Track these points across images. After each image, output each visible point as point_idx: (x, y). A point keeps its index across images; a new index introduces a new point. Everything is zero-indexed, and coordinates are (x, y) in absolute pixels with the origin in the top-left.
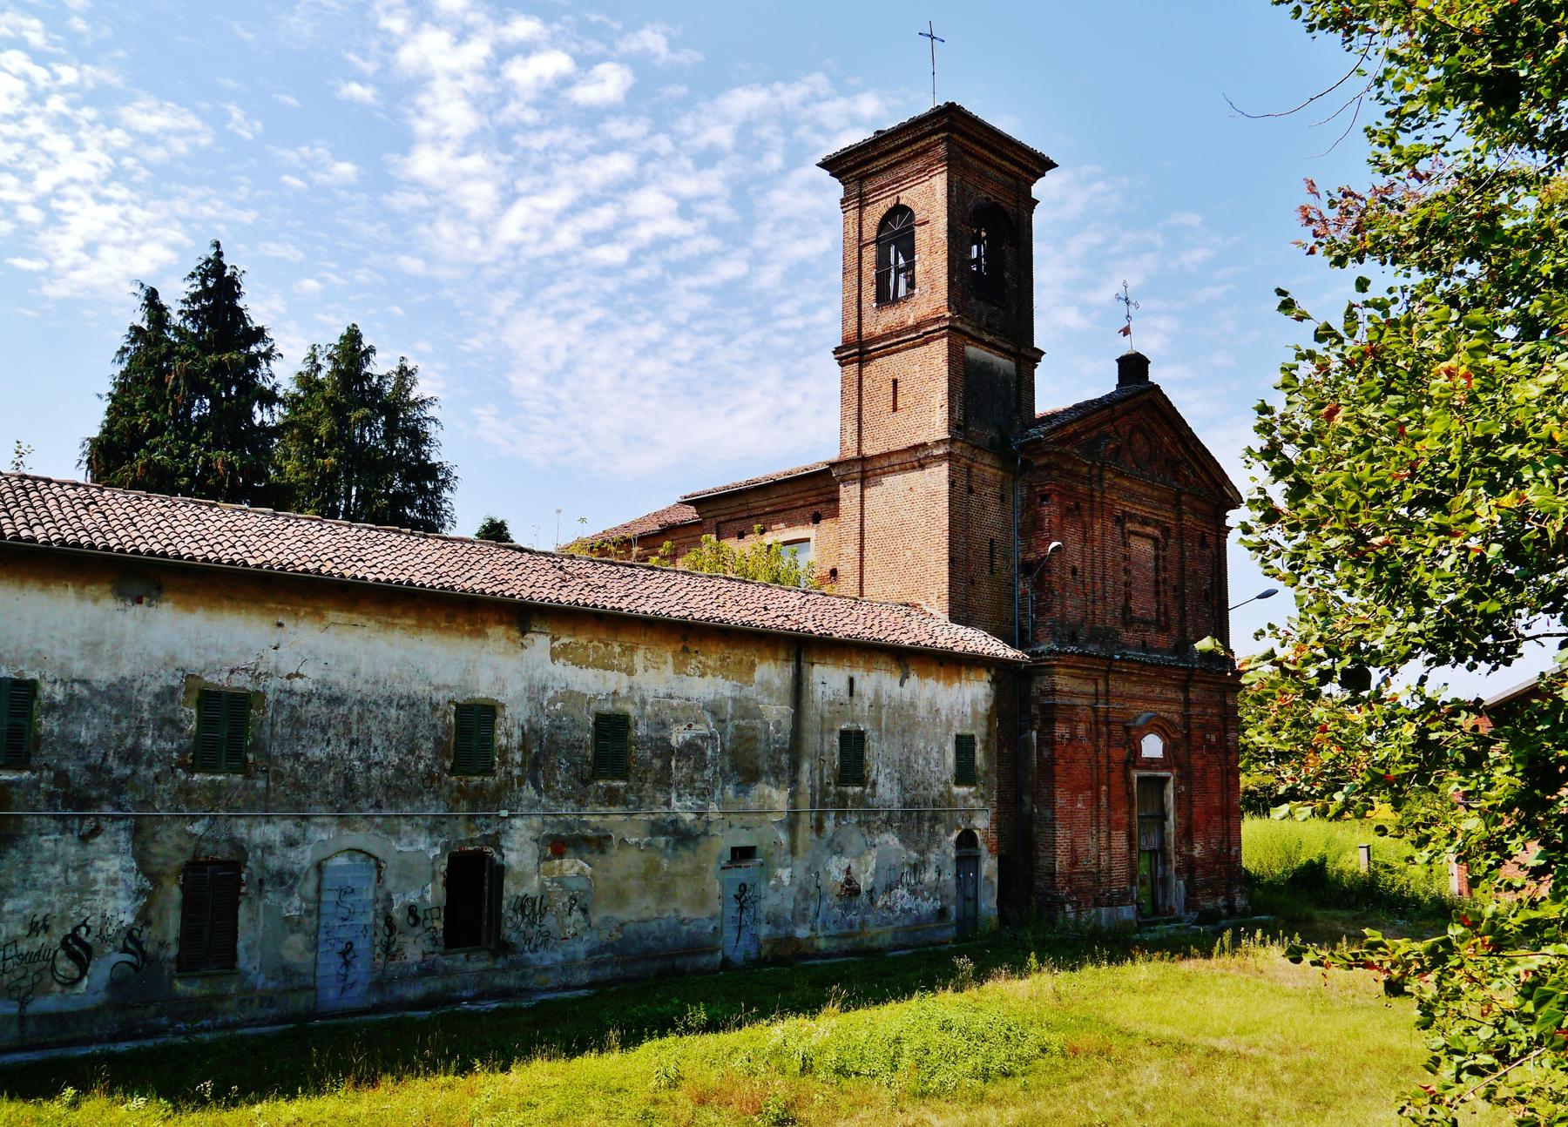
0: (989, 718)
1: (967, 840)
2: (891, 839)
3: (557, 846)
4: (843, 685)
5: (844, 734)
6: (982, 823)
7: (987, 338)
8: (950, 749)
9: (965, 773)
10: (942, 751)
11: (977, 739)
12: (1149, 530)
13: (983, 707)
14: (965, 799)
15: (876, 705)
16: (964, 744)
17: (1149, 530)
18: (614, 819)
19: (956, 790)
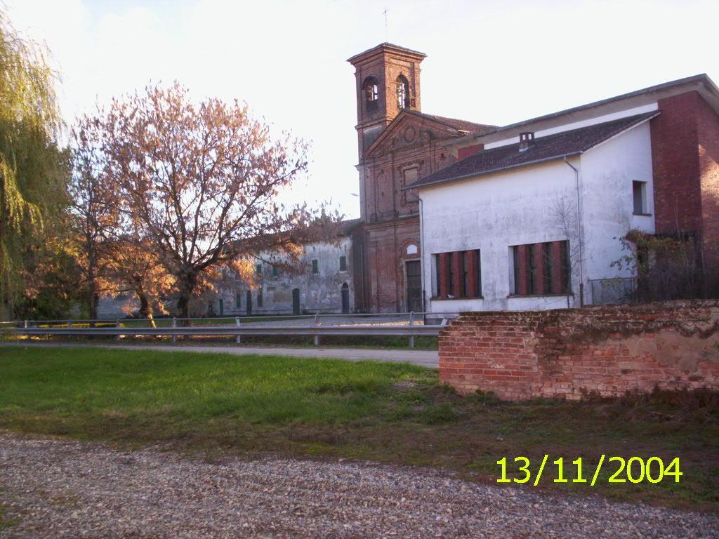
0: (350, 251)
1: (345, 285)
2: (323, 286)
3: (269, 289)
4: (312, 249)
5: (313, 261)
6: (348, 282)
7: (368, 124)
8: (339, 261)
9: (343, 267)
10: (336, 262)
11: (347, 257)
12: (414, 165)
13: (348, 248)
14: (343, 274)
15: (320, 253)
16: (343, 259)
17: (414, 165)
18: (276, 283)
19: (341, 272)
